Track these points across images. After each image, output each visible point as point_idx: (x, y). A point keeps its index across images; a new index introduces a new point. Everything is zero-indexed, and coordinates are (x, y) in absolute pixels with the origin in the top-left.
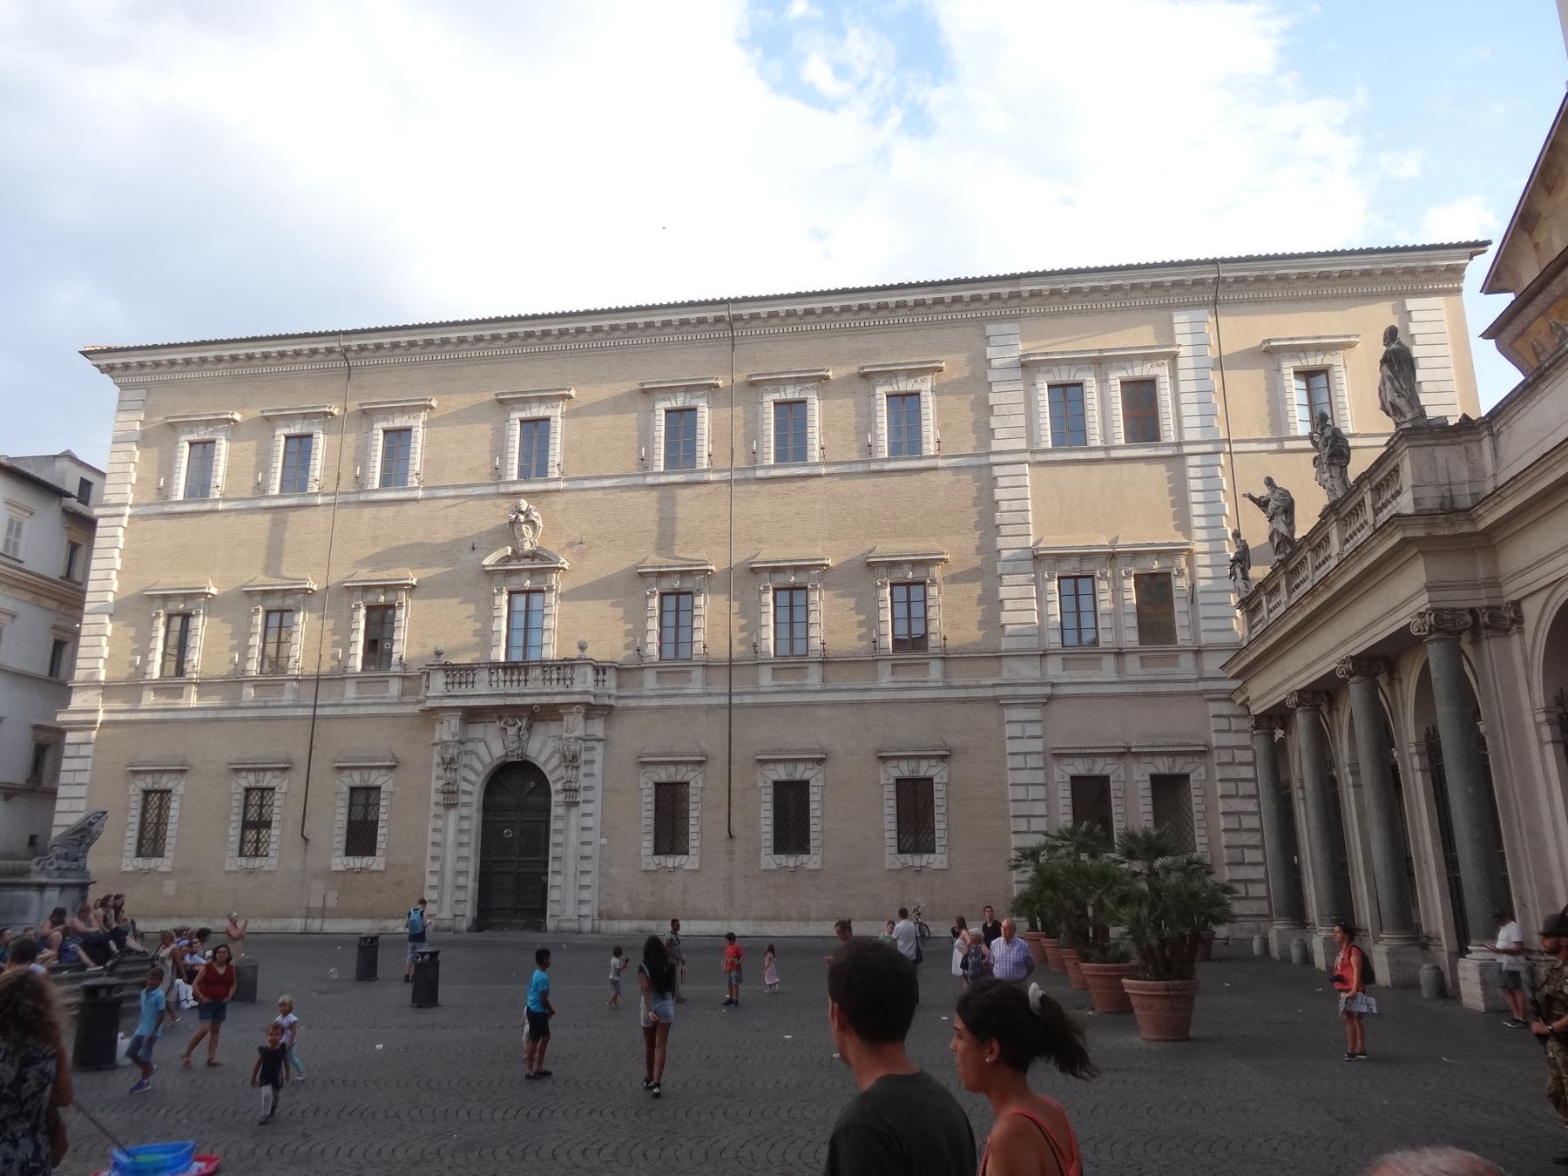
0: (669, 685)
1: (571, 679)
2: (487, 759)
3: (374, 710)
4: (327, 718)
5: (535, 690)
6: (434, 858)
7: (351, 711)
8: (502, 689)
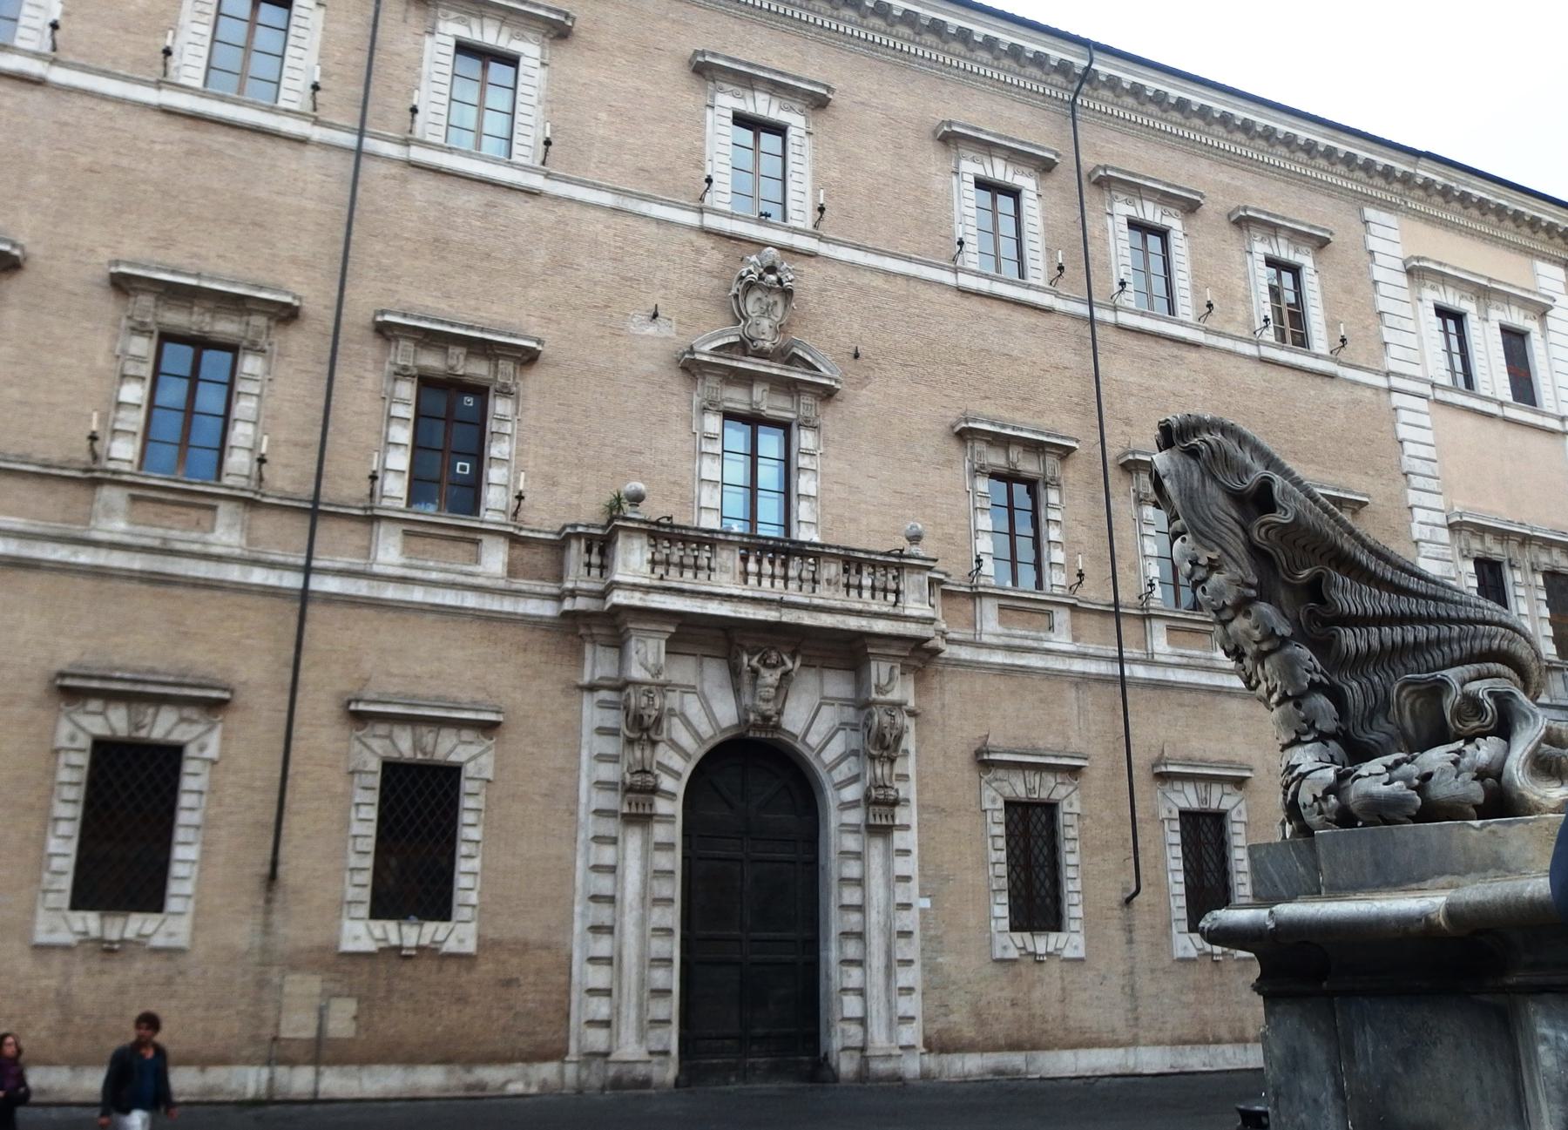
0: (1020, 633)
1: (897, 592)
2: (706, 729)
3: (449, 598)
4: (330, 599)
5: (828, 603)
6: (596, 929)
7: (391, 592)
8: (767, 589)
